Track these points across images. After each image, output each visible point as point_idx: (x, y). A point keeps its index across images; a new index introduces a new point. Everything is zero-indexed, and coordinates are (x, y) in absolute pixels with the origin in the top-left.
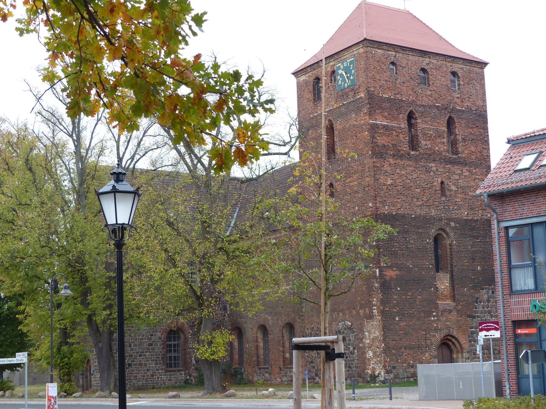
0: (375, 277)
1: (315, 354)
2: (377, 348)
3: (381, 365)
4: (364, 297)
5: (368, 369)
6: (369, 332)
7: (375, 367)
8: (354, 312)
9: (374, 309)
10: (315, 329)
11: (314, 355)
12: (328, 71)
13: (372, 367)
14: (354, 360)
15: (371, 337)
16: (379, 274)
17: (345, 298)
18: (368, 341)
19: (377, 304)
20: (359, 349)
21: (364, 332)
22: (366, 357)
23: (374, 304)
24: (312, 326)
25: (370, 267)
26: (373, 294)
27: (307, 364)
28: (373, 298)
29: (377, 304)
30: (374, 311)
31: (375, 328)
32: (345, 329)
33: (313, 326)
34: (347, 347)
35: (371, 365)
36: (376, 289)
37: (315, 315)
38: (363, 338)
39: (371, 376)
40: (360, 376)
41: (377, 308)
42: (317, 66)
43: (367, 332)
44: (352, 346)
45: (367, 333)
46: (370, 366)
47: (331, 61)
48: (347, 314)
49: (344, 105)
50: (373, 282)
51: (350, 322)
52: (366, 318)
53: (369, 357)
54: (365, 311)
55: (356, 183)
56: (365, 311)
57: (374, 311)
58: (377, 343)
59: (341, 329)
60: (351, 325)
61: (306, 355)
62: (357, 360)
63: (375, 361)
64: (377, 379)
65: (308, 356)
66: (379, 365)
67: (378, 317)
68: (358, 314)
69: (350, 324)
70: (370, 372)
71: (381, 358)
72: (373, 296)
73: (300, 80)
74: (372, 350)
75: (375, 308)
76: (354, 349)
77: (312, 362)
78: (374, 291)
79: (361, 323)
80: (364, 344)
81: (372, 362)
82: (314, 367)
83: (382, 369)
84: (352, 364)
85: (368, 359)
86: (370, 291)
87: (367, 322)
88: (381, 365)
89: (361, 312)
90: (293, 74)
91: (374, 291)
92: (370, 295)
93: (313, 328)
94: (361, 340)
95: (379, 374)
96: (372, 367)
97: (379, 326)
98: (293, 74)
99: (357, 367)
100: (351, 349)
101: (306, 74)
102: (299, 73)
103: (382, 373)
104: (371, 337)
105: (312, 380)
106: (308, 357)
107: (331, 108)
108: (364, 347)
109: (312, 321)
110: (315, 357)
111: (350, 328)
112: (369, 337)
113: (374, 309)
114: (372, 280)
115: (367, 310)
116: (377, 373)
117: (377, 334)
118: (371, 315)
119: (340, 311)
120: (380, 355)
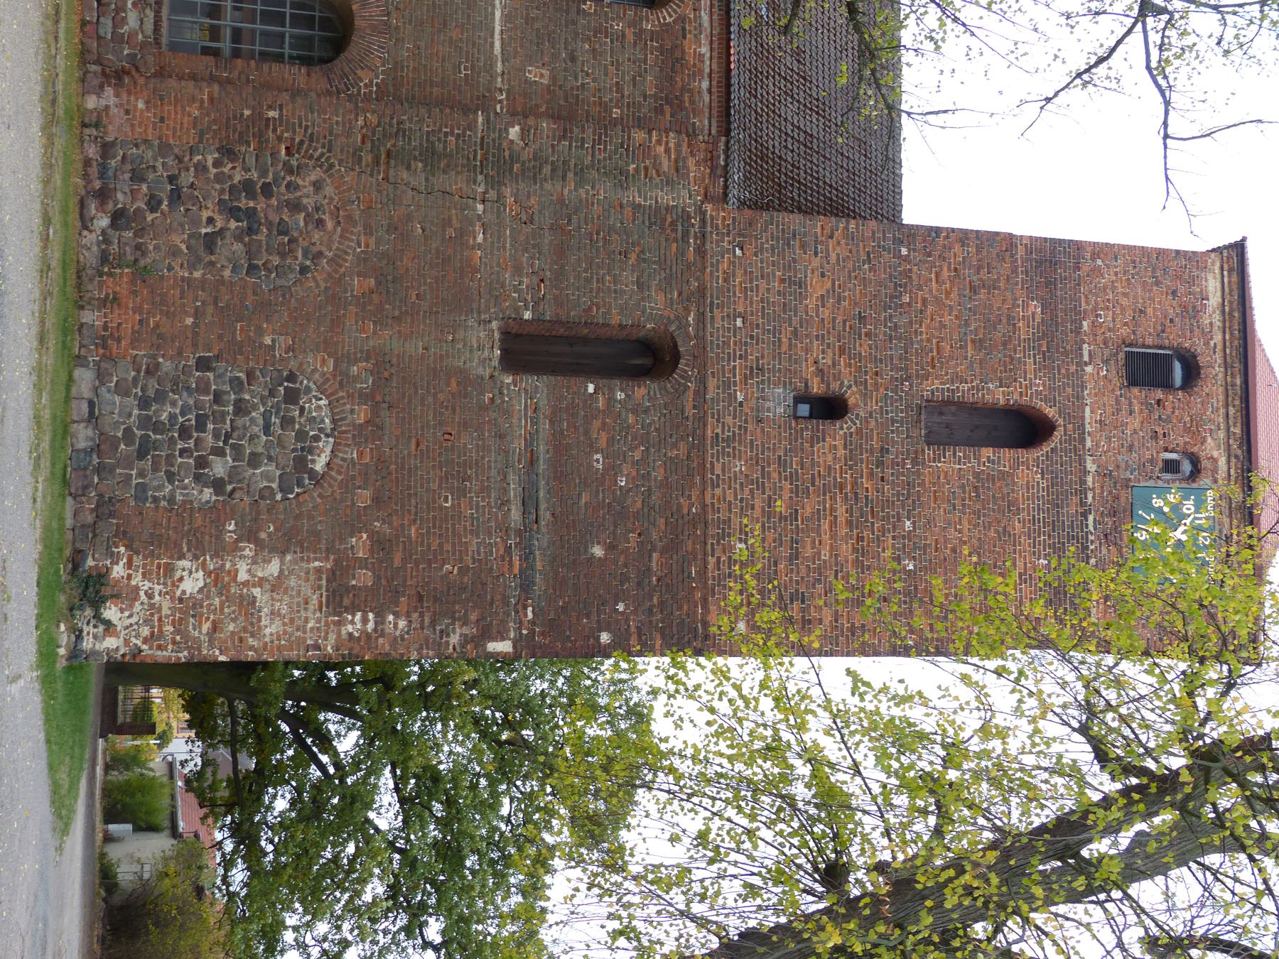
0: (486, 634)
1: (211, 221)
2: (215, 628)
3: (145, 641)
4: (417, 563)
5: (129, 564)
6: (276, 585)
7: (137, 607)
8: (364, 497)
9: (365, 621)
10: (316, 236)
11: (205, 214)
12: (1204, 441)
13: (137, 588)
14: (170, 477)
15: (256, 592)
16: (496, 656)
17: (423, 447)
18: (243, 576)
19: (382, 635)
20: (216, 515)
21: (283, 553)
22: (180, 558)
23: (383, 623)
24: (326, 217)
25: (525, 608)
26: (422, 615)
27: (171, 161)
28: (408, 615)
29: (382, 635)
30: (359, 616)
31: (292, 620)
32: (301, 435)
33: (330, 225)
34: (228, 436)
35: (147, 584)
36: (442, 631)
37: (372, 241)
38: (259, 544)
39: (101, 577)
40: (105, 508)
41: (368, 636)
42: (1233, 385)
43: (281, 571)
44: (233, 473)
45: (274, 568)
46: (144, 575)
47: (1233, 460)
48: (361, 454)
49: (1085, 515)
50: (465, 623)
51: (328, 464)
52: (333, 571)
53: (178, 574)
54: (363, 564)
55: (825, 555)
56: (363, 564)
57: (359, 616)
58: (231, 627)
59: (302, 409)
60: (312, 474)
61: (210, 162)
62: (171, 500)
63: (160, 609)
64: (89, 612)
65: (205, 168)
66: (145, 631)
67: (332, 637)
68: (354, 524)
69: (320, 465)
70: (118, 571)
71: (174, 642)
72: (415, 615)
73: (1210, 277)
74: (208, 597)
75: (370, 626)
76: (218, 485)
77: (176, 196)
78: (433, 623)
79: (317, 534)
80: (235, 549)
81: (157, 588)
82: (153, 204)
83: (127, 642)
84: (155, 469)
85: (170, 569)
86: (436, 600)
87: (318, 571)
88: (145, 641)
89: (360, 544)
90: (1239, 248)
91: (433, 623)
92: (420, 598)
93: (320, 223)
94: (250, 534)
95: (108, 624)
96: (137, 588)
97: (298, 638)
98: (1239, 248)
99: (142, 488)
100: (219, 468)
101: (1223, 312)
102: (1235, 278)
103: (111, 643)
104: (256, 592)
105: (97, 184)
106: (201, 168)
107: (1089, 444)
108: (219, 551)
109: (349, 218)
110: (196, 222)
111: (301, 463)
112: (261, 582)
113: (365, 621)
114: (473, 617)
115: (363, 578)
116: (111, 612)
117: (271, 629)
118: (346, 602)
119: (375, 411)
120: (186, 636)
